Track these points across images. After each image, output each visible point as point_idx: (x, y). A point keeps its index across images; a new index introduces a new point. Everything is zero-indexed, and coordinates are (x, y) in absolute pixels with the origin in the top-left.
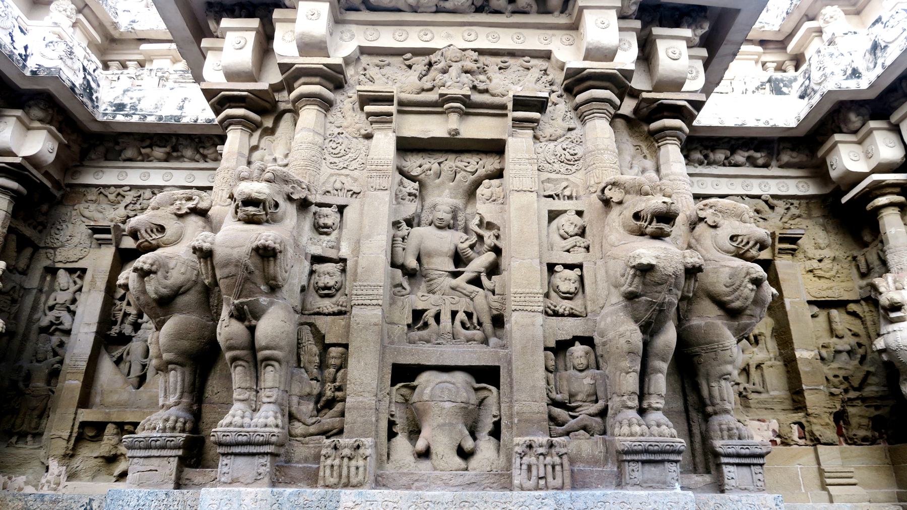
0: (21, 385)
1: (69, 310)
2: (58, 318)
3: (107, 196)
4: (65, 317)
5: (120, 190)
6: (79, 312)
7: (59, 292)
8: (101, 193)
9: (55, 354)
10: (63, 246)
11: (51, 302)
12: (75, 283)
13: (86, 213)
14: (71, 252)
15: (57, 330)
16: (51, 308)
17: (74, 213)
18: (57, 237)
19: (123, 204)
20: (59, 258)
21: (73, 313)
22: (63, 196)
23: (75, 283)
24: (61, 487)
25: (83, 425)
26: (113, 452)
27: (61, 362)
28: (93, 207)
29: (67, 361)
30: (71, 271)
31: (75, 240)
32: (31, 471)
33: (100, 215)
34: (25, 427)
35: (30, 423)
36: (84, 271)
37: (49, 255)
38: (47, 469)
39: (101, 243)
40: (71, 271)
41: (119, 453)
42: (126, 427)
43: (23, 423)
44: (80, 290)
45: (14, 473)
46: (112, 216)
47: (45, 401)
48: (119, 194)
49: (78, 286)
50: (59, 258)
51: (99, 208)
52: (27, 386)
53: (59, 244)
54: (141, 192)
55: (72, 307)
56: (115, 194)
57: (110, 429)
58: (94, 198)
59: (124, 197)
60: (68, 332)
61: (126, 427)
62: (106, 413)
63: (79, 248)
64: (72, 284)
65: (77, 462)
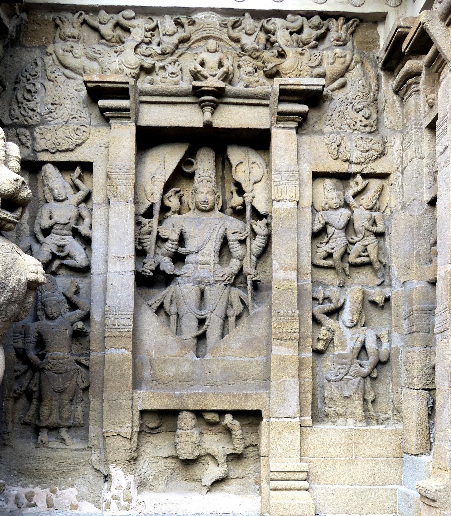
0: (32, 355)
1: (76, 233)
2: (61, 248)
3: (96, 30)
4: (75, 247)
5: (119, 17)
6: (97, 237)
7: (53, 203)
8: (85, 22)
9: (73, 306)
10: (44, 122)
11: (46, 223)
12: (76, 188)
13: (69, 60)
14: (60, 134)
15: (62, 266)
16: (47, 232)
17: (49, 60)
18: (31, 105)
19: (131, 41)
20: (41, 144)
21: (87, 241)
22: (19, 29)
23: (76, 188)
24: (133, 504)
25: (143, 413)
26: (196, 454)
27: (87, 318)
28: (79, 49)
29: (96, 317)
30: (65, 167)
31: (63, 112)
32: (81, 481)
33: (95, 65)
34: (54, 419)
35: (60, 413)
36: (87, 167)
37: (24, 139)
38: (107, 478)
39: (107, 117)
40: (65, 167)
41: (203, 452)
42: (208, 417)
43: (51, 413)
44: (88, 198)
45: (57, 484)
46: (115, 66)
47: (74, 379)
48: (117, 25)
49: (81, 194)
50: (41, 144)
51: (90, 51)
52: (42, 357)
53: (37, 119)
54: (157, 20)
55: (83, 229)
56: (110, 25)
57: (186, 420)
58: (75, 32)
59: (127, 30)
60: (85, 271)
61: (208, 417)
62: (177, 397)
63: (73, 125)
64: (71, 191)
65: (144, 467)
